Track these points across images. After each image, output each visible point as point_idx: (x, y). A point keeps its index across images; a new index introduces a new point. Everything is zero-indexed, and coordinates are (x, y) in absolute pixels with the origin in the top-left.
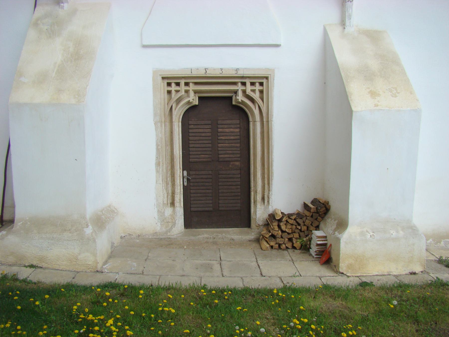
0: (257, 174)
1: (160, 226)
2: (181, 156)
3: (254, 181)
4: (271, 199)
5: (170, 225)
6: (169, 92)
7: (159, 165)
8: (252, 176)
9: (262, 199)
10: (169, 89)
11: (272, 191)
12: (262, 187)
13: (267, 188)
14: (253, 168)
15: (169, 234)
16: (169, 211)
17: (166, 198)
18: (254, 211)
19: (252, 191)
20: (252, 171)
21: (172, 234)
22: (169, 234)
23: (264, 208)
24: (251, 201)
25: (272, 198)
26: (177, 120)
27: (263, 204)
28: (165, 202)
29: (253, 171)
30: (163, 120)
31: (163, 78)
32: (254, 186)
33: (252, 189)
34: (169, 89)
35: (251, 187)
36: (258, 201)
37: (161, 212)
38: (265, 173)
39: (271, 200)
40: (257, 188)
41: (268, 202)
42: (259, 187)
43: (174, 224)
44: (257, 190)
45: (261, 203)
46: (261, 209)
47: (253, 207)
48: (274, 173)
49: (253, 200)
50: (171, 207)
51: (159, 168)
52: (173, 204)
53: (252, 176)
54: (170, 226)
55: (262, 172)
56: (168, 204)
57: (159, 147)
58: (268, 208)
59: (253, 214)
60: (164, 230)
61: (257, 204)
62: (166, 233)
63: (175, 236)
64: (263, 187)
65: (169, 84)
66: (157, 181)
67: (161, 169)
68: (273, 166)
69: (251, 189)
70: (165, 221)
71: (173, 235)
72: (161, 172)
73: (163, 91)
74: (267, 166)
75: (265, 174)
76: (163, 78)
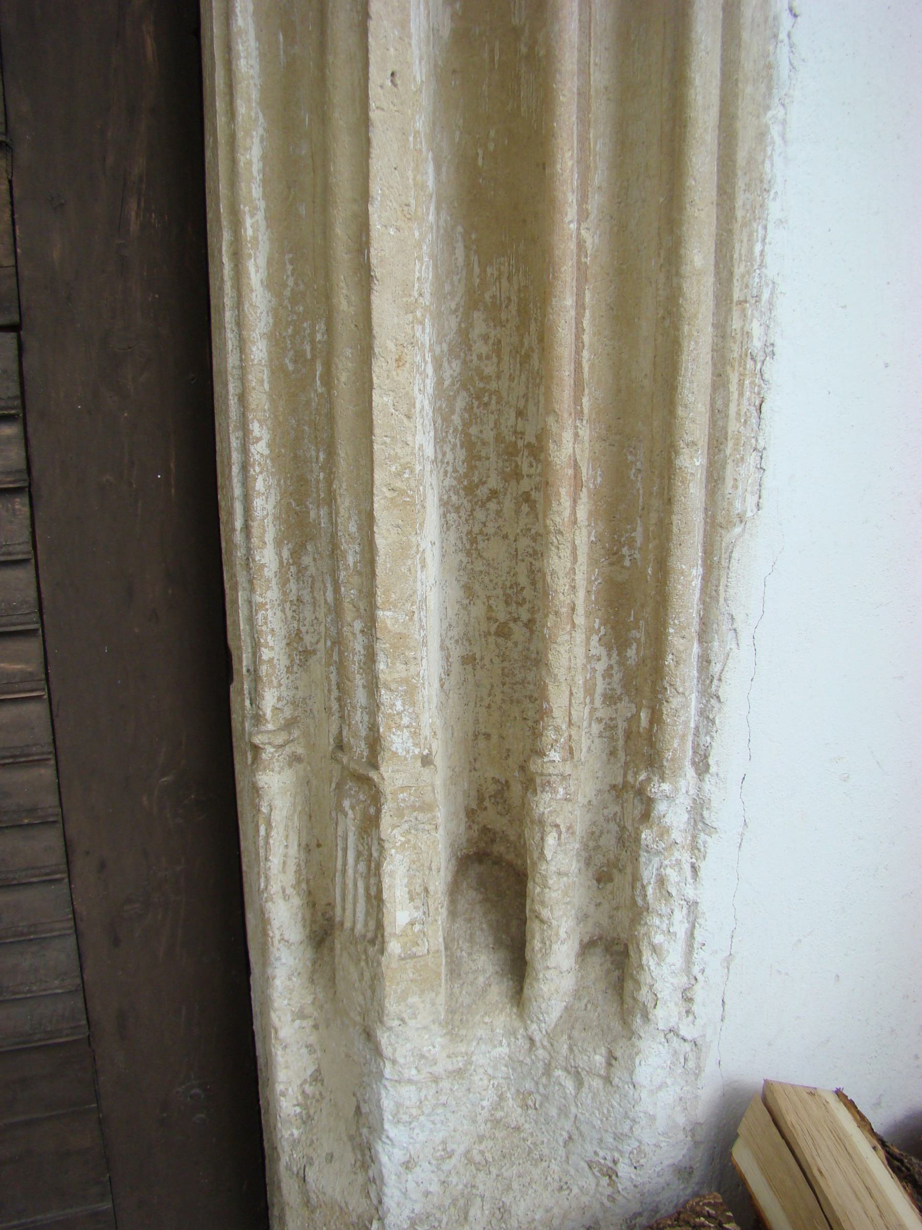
0: (378, 399)
3: (296, 554)
4: (679, 916)
8: (260, 449)
9: (454, 890)
11: (702, 766)
12: (456, 652)
13: (590, 691)
14: (273, 284)
18: (317, 1078)
19: (268, 753)
20: (259, 351)
23: (513, 1062)
24: (265, 922)
25: (692, 906)
27: (498, 991)
29: (275, 339)
32: (294, 640)
33: (269, 700)
35: (243, 661)
36: (394, 947)
38: (566, 373)
39: (680, 927)
40: (374, 707)
41: (597, 962)
42: (410, 693)
44: (375, 743)
45: (455, 970)
46: (459, 1073)
47: (301, 1015)
48: (773, 369)
49: (296, 901)
53: (260, 449)
55: (452, 370)
58: (608, 1080)
59: (307, 1120)
61: (392, 1006)
64: (469, 660)
68: (757, 211)
69: (241, 704)
74: (595, 202)
75: (564, 395)
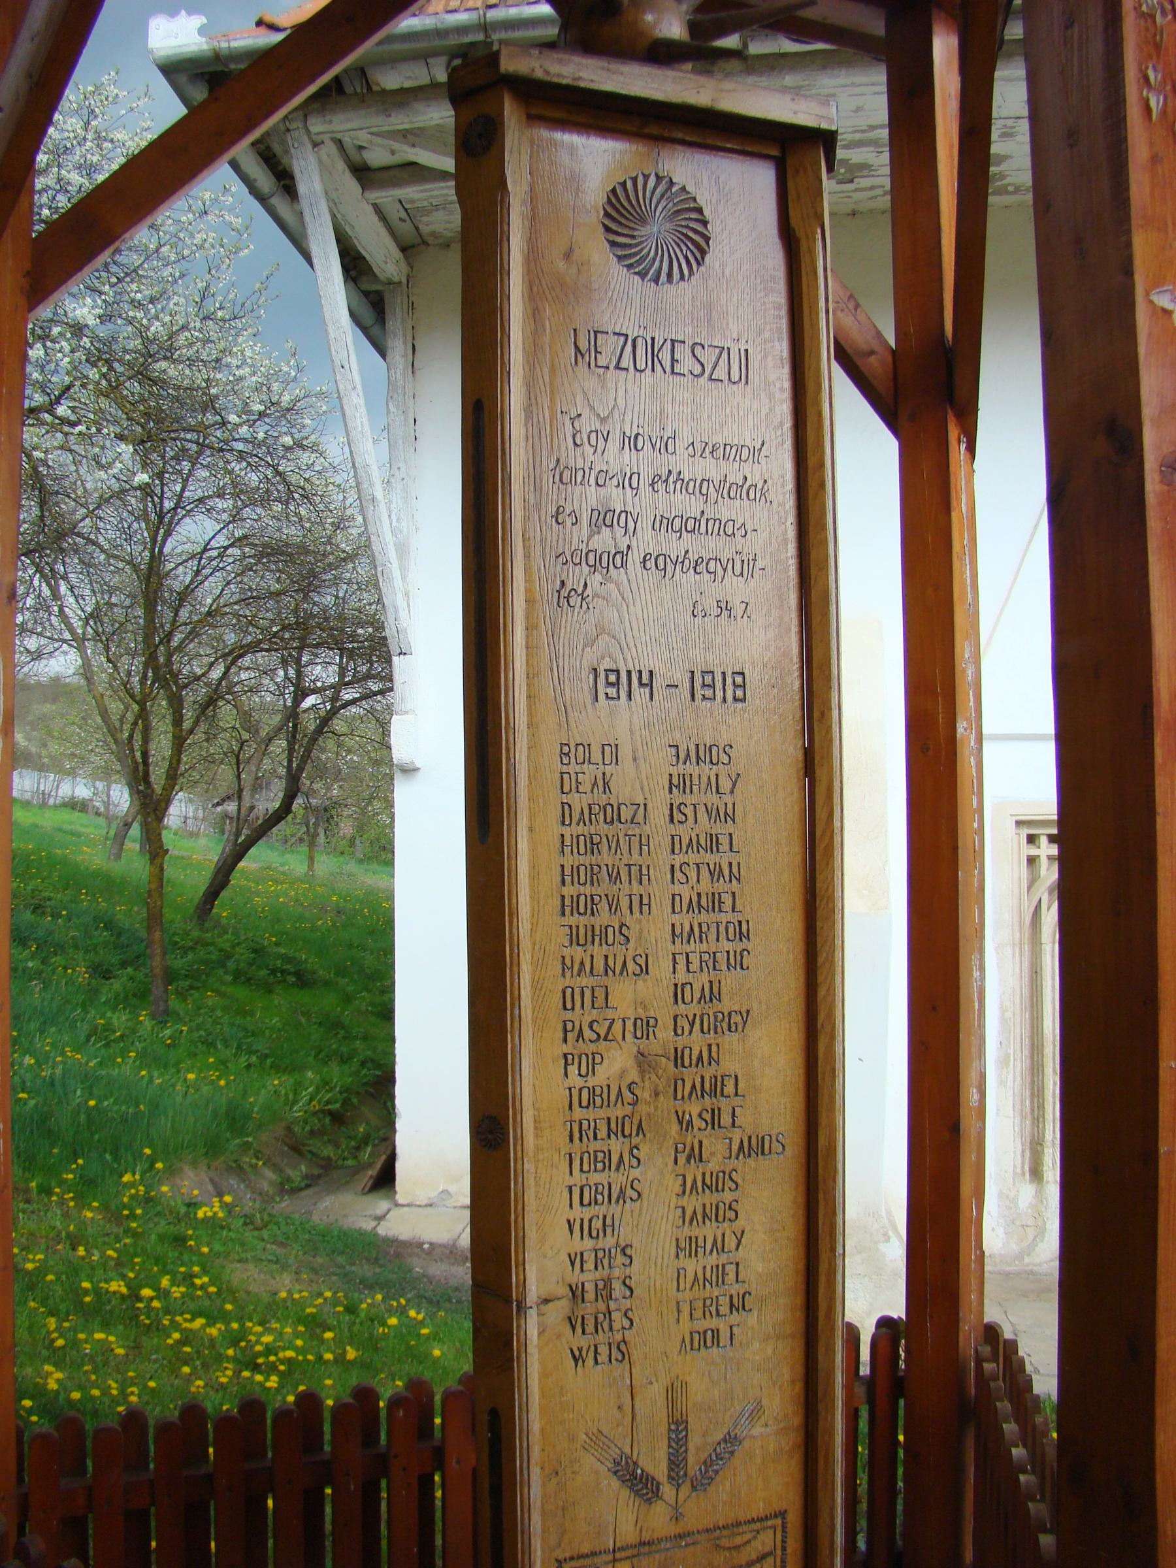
1: (1002, 1235)
2: (1058, 1038)
5: (1031, 1233)
6: (1032, 860)
7: (1007, 1065)
10: (1033, 851)
15: (1027, 1260)
16: (1026, 1192)
17: (1019, 1157)
21: (1037, 1260)
22: (1027, 1260)
26: (1050, 940)
28: (1019, 1170)
30: (1017, 940)
31: (1019, 823)
34: (1033, 851)
37: (1007, 1197)
43: (1041, 1231)
50: (1031, 1181)
51: (1005, 1071)
52: (1036, 1173)
54: (1031, 1238)
56: (1023, 1174)
57: (1008, 1015)
60: (1014, 1247)
62: (1020, 1256)
63: (1046, 1266)
65: (1031, 839)
66: (998, 1110)
67: (1011, 1077)
70: (1018, 1223)
71: (1040, 1264)
72: (1010, 1084)
73: (1016, 857)
76: (1019, 823)
